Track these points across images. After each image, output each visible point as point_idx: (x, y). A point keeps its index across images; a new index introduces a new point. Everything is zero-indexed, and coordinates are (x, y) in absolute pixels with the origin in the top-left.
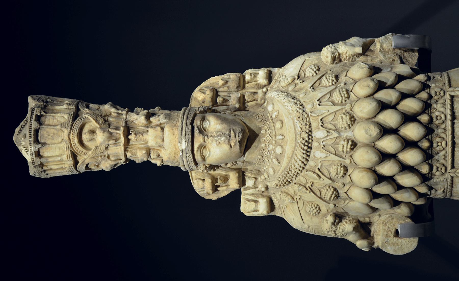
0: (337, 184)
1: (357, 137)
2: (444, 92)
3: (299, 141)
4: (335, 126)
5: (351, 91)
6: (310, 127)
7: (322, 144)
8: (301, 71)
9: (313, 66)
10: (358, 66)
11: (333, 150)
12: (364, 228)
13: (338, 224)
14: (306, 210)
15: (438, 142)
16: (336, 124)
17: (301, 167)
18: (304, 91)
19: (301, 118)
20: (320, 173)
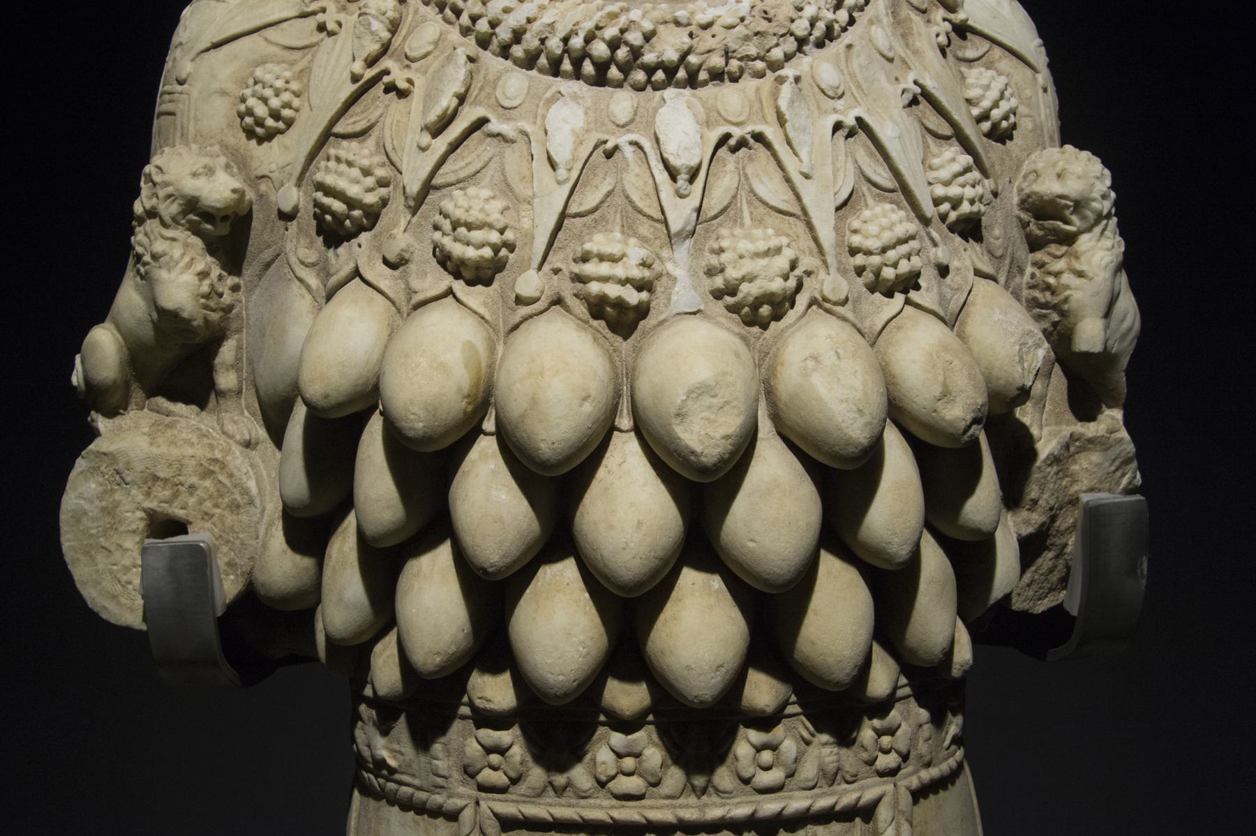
0: (403, 223)
1: (665, 334)
2: (892, 773)
3: (635, 14)
4: (723, 211)
5: (908, 302)
6: (717, 76)
7: (623, 139)
8: (986, 45)
9: (1013, 102)
10: (1029, 333)
11: (588, 199)
12: (181, 365)
13: (196, 231)
14: (261, 62)
15: (637, 755)
16: (737, 220)
17: (494, 24)
18: (900, 50)
19: (763, 26)
20: (456, 129)
